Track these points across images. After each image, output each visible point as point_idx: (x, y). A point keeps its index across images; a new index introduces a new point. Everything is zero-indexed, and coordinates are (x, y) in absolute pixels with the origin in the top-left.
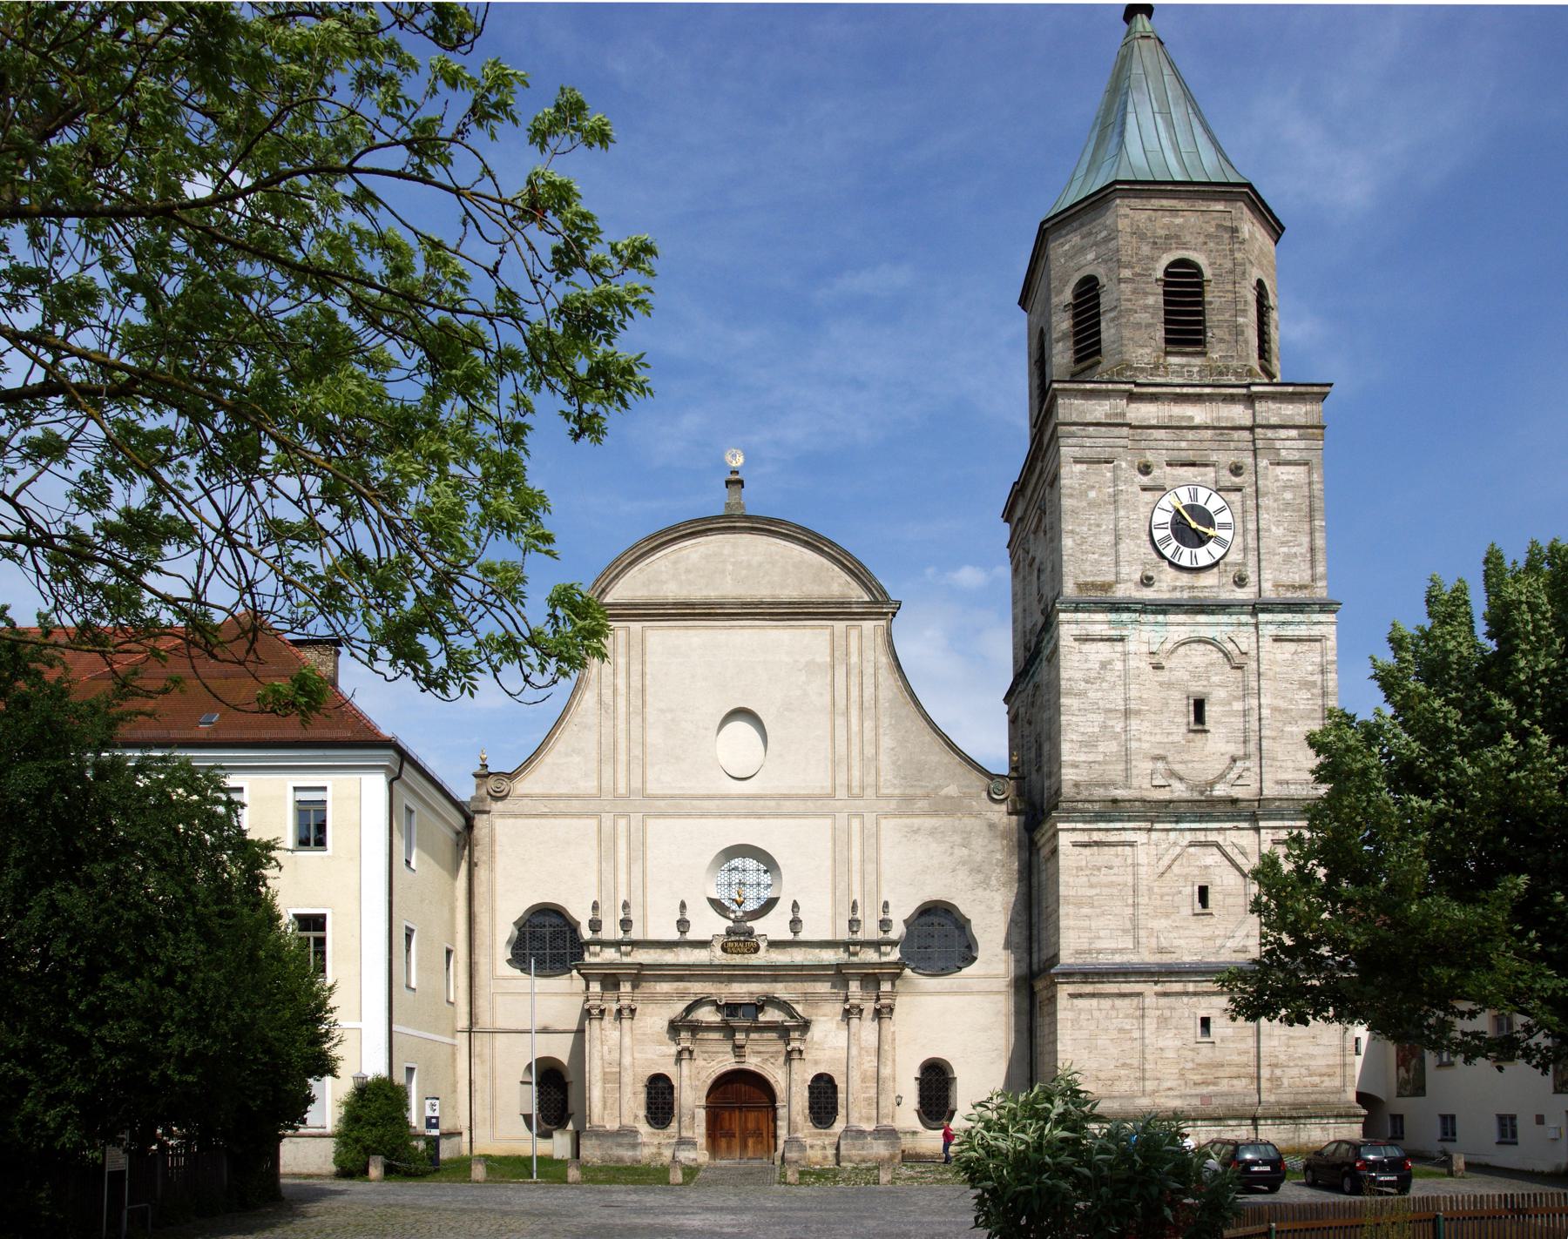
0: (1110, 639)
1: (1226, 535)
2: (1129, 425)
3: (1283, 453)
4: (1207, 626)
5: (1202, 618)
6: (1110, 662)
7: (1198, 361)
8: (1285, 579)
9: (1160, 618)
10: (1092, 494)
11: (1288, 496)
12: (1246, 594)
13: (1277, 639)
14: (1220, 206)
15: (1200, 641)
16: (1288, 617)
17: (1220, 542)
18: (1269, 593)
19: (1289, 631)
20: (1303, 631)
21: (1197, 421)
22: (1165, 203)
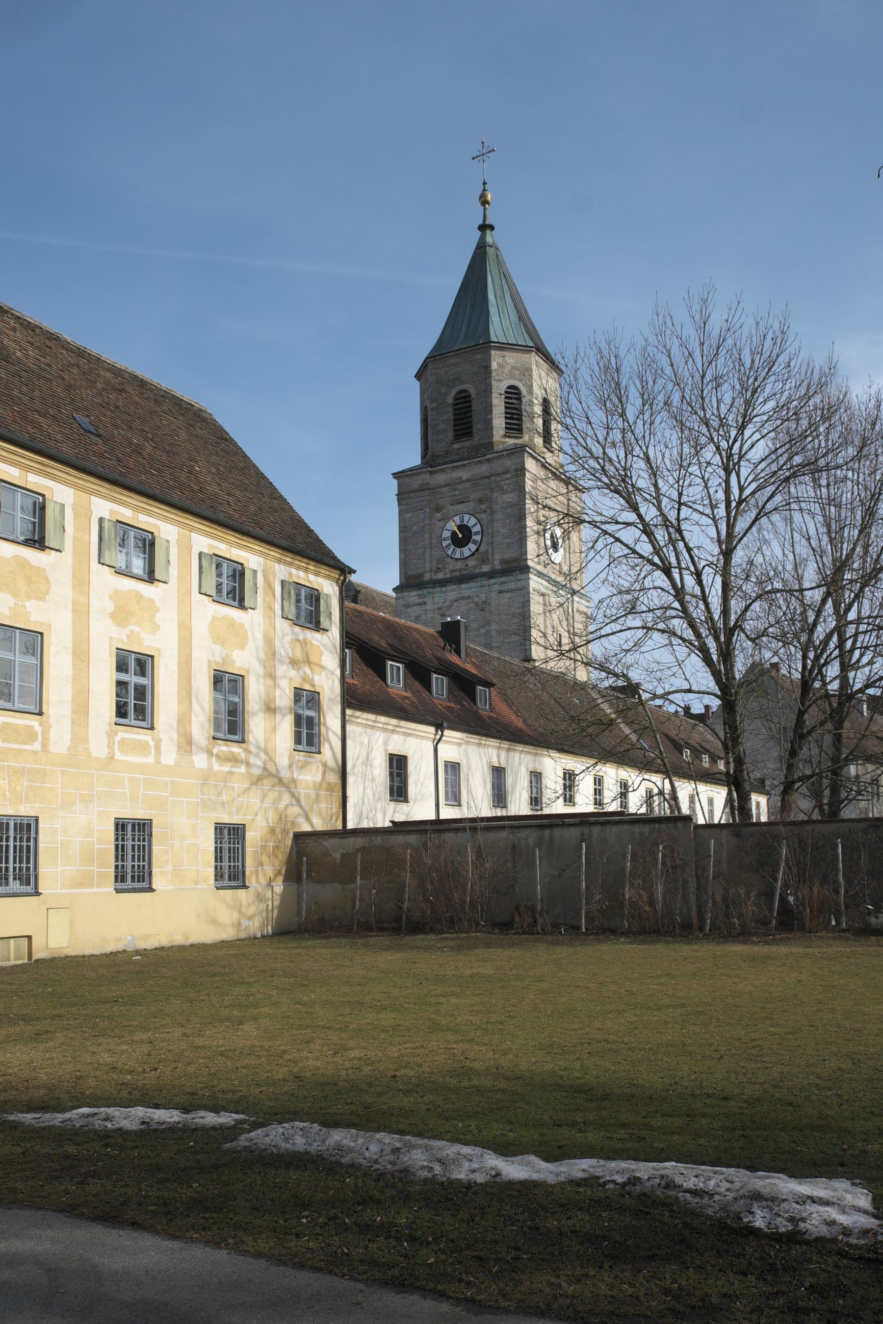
0: (419, 604)
1: (478, 538)
2: (430, 489)
3: (505, 487)
4: (466, 589)
5: (463, 586)
6: (420, 616)
7: (468, 444)
8: (507, 556)
9: (443, 589)
10: (415, 528)
11: (509, 510)
12: (485, 568)
13: (500, 592)
14: (480, 356)
15: (463, 598)
16: (504, 579)
17: (475, 542)
18: (498, 566)
19: (506, 587)
20: (512, 586)
21: (464, 478)
22: (453, 361)
